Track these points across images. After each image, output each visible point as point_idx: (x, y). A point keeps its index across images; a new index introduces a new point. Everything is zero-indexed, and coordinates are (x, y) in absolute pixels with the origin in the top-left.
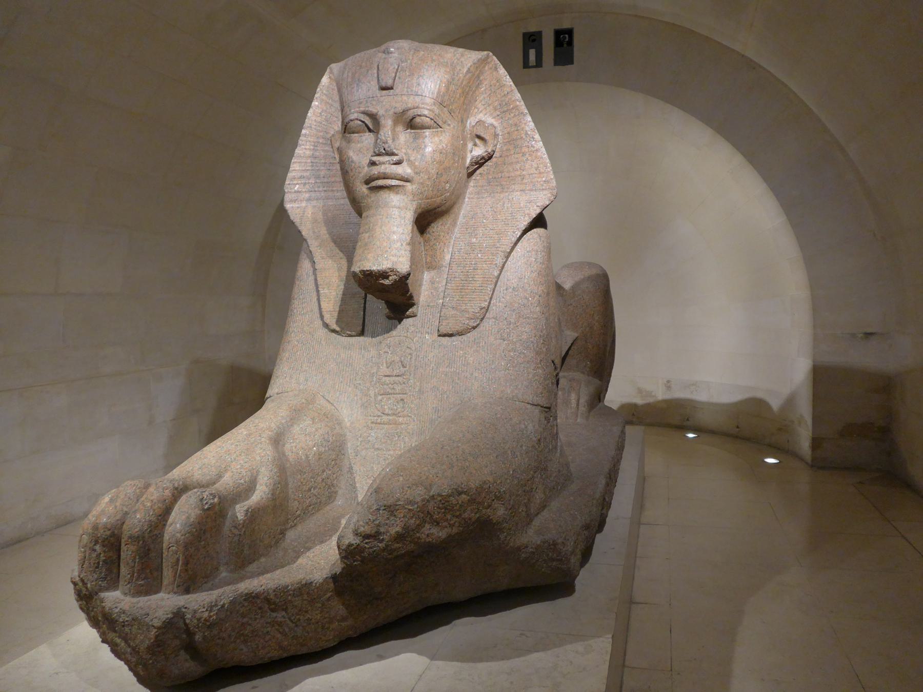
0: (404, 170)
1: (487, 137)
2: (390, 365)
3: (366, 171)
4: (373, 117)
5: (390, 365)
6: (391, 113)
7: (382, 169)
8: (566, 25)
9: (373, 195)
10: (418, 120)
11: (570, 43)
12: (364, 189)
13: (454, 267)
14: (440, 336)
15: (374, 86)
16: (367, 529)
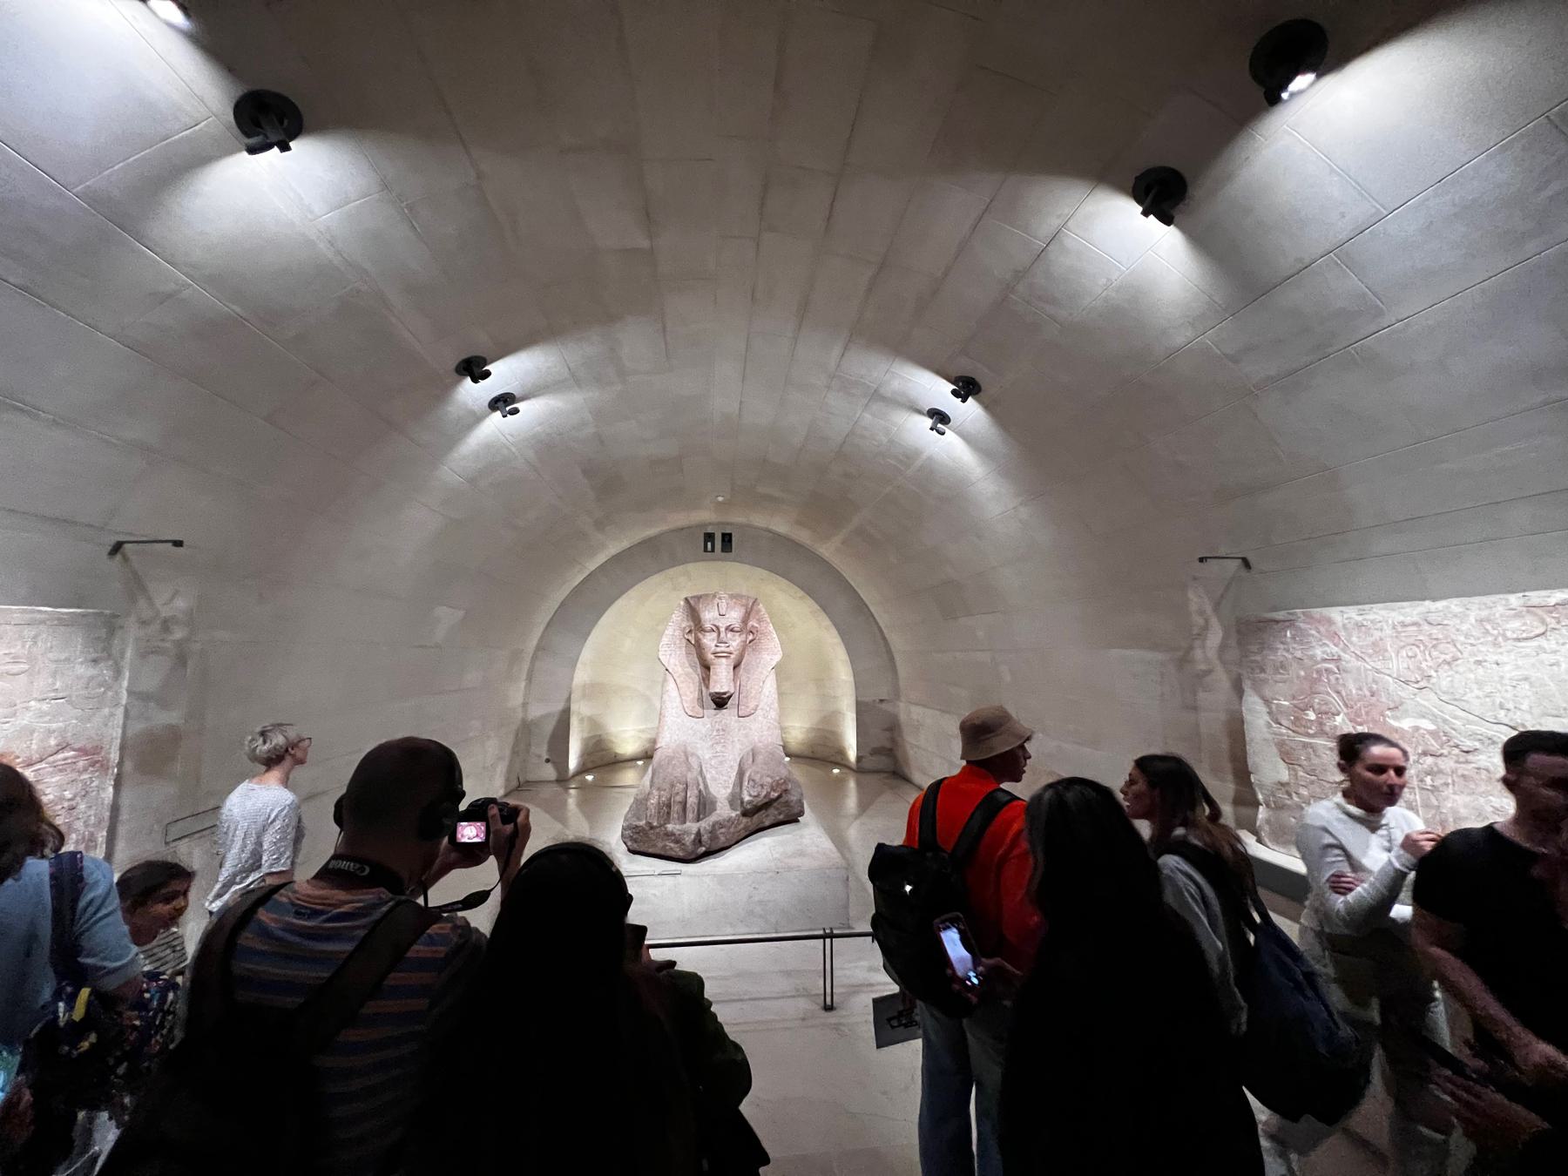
0: (731, 648)
1: (754, 631)
2: (718, 730)
3: (713, 648)
4: (718, 628)
5: (718, 730)
6: (725, 626)
7: (723, 649)
8: (728, 531)
9: (716, 659)
10: (735, 629)
11: (730, 541)
12: (712, 657)
13: (742, 688)
14: (739, 717)
15: (717, 613)
16: (755, 794)
